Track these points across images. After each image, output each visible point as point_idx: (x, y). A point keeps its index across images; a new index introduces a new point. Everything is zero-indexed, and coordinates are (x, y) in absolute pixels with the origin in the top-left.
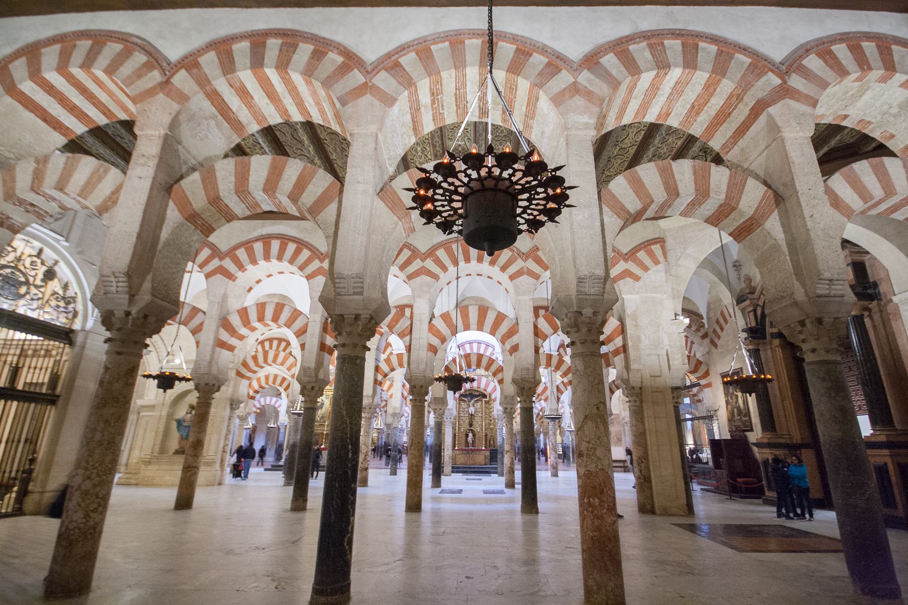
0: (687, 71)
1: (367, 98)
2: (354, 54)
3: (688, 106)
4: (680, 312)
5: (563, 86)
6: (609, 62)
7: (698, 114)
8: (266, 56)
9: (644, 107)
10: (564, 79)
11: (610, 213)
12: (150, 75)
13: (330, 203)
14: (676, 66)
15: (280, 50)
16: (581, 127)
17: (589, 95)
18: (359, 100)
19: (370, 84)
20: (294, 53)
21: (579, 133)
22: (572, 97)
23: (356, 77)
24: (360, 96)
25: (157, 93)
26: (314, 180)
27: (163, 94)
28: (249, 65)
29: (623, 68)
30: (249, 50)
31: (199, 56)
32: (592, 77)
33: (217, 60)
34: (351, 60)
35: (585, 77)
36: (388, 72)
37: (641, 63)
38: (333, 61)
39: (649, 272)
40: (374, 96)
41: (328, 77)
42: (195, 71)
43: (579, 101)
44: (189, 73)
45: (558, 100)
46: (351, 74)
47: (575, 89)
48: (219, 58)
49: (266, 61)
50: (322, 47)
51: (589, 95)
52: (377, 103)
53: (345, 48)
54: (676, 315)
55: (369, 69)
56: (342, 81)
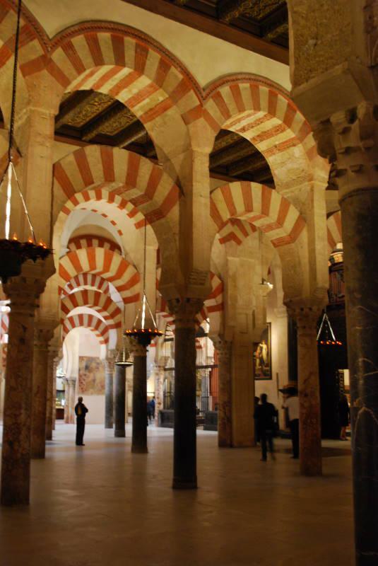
2: (193, 78)
8: (126, 55)
12: (31, 44)
15: (136, 52)
18: (197, 121)
23: (192, 99)
24: (197, 117)
27: (47, 70)
30: (110, 42)
31: (73, 37)
33: (87, 46)
34: (189, 82)
38: (176, 76)
41: (174, 92)
42: (70, 52)
48: (88, 43)
49: (126, 59)
50: (168, 60)
52: (208, 127)
53: (186, 68)
56: (184, 99)
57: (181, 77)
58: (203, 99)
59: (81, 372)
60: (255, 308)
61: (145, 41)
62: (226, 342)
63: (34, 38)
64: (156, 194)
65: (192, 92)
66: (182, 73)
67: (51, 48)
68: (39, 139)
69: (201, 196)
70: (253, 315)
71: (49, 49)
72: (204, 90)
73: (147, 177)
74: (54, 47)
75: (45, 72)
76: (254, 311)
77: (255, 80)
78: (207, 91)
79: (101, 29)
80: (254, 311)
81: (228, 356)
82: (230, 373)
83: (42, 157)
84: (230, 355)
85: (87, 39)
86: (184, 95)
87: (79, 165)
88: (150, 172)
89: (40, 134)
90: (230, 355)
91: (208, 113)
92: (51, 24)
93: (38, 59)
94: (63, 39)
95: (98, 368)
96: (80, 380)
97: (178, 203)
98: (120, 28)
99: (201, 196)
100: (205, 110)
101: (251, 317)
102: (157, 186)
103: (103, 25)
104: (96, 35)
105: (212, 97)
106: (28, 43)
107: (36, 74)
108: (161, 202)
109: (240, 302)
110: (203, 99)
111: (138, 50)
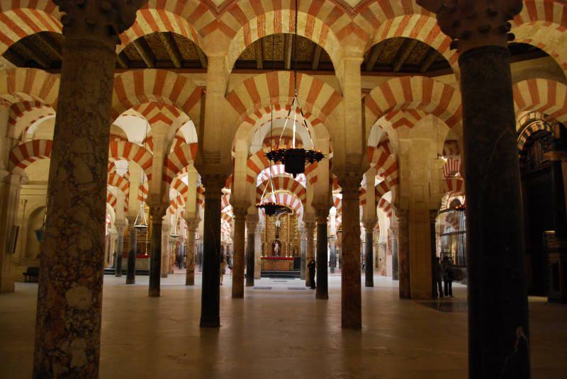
0: (423, 16)
1: (217, 32)
3: (429, 32)
4: (441, 153)
5: (344, 25)
6: (374, 8)
7: (434, 37)
9: (401, 30)
10: (345, 20)
11: (370, 112)
13: (196, 102)
14: (417, 13)
16: (354, 55)
17: (360, 32)
18: (212, 33)
19: (219, 21)
21: (352, 59)
22: (350, 33)
23: (209, 16)
26: (185, 87)
29: (383, 13)
32: (363, 19)
35: (358, 19)
36: (231, 13)
37: (395, 10)
39: (421, 120)
40: (221, 30)
43: (353, 37)
45: (340, 35)
46: (206, 14)
47: (352, 27)
51: (360, 32)
52: (224, 35)
54: (438, 155)
55: (218, 10)
56: (200, 19)
58: (217, 14)
62: (402, 210)
64: (180, 97)
65: (209, 11)
72: (219, 7)
73: (172, 86)
81: (405, 222)
82: (408, 236)
88: (175, 82)
91: (225, 25)
100: (221, 22)
101: (428, 188)
105: (229, 11)
108: (184, 102)
109: (414, 176)
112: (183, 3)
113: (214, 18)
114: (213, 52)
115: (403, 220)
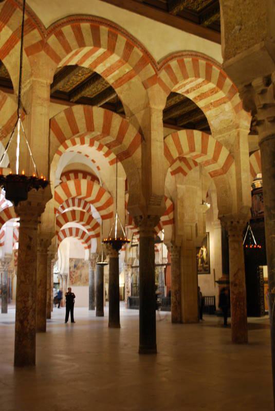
12: (32, 32)
18: (154, 86)
20: (116, 41)
23: (150, 70)
24: (153, 84)
25: (41, 51)
28: (92, 43)
30: (90, 30)
31: (63, 26)
33: (73, 33)
34: (147, 57)
38: (138, 54)
41: (136, 65)
42: (61, 37)
44: (58, 39)
48: (74, 31)
50: (132, 43)
52: (162, 90)
56: (143, 70)
57: (141, 54)
58: (157, 70)
59: (71, 270)
60: (197, 222)
61: (115, 29)
62: (176, 247)
63: (35, 28)
64: (124, 140)
65: (150, 64)
66: (142, 51)
67: (47, 35)
68: (39, 101)
69: (157, 141)
70: (196, 227)
71: (46, 36)
72: (158, 63)
73: (118, 128)
74: (49, 34)
75: (43, 53)
76: (196, 224)
77: (196, 56)
78: (161, 64)
79: (83, 20)
80: (196, 224)
81: (178, 257)
82: (180, 268)
83: (41, 114)
84: (180, 257)
85: (73, 28)
86: (144, 67)
87: (68, 120)
89: (40, 98)
90: (180, 257)
92: (47, 18)
93: (37, 43)
94: (56, 28)
95: (83, 266)
96: (70, 276)
97: (140, 146)
98: (97, 19)
99: (157, 141)
100: (159, 78)
102: (125, 133)
103: (84, 17)
104: (80, 25)
105: (164, 69)
106: (30, 31)
107: (37, 54)
108: (128, 145)
109: (186, 218)
110: (157, 70)
111: (110, 36)
112: (130, 51)
113: (153, 72)
114: (155, 104)
115: (176, 255)
